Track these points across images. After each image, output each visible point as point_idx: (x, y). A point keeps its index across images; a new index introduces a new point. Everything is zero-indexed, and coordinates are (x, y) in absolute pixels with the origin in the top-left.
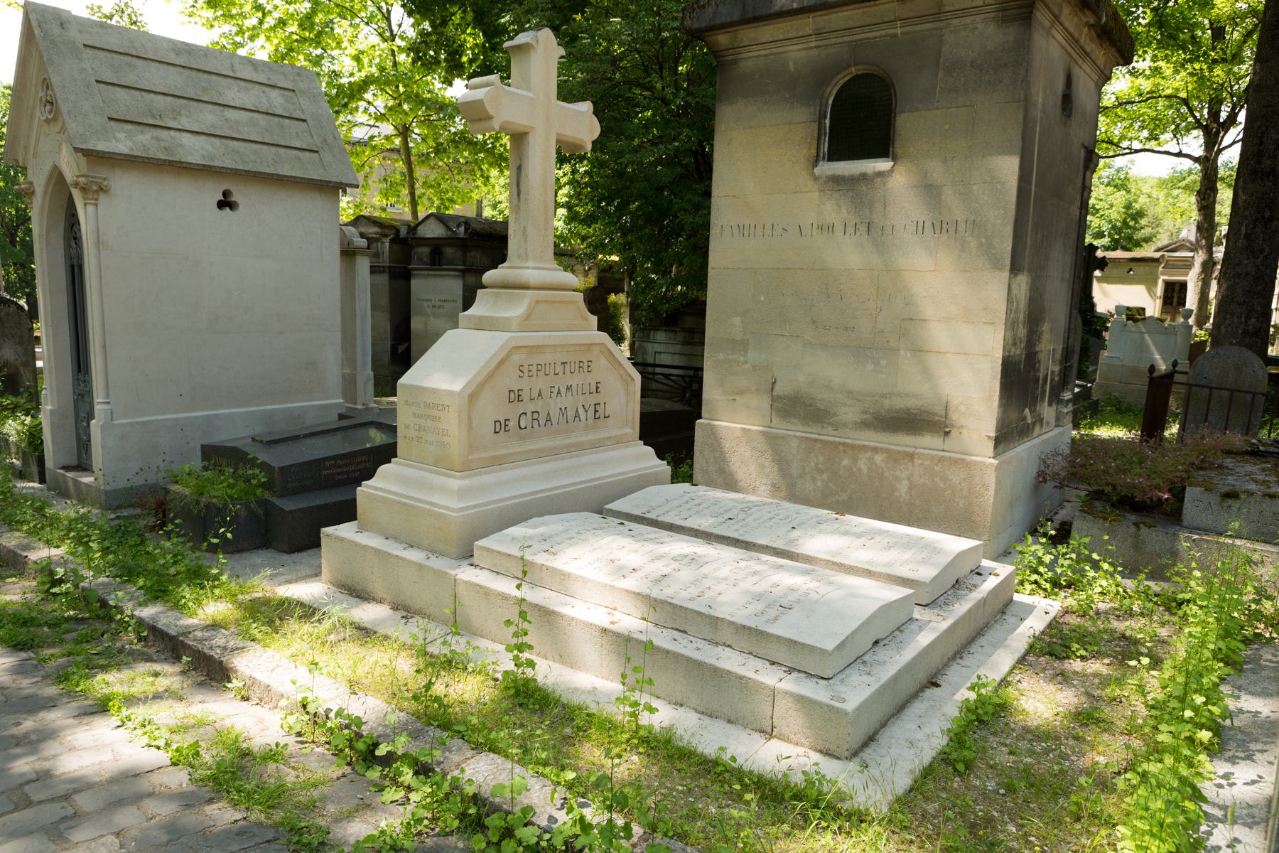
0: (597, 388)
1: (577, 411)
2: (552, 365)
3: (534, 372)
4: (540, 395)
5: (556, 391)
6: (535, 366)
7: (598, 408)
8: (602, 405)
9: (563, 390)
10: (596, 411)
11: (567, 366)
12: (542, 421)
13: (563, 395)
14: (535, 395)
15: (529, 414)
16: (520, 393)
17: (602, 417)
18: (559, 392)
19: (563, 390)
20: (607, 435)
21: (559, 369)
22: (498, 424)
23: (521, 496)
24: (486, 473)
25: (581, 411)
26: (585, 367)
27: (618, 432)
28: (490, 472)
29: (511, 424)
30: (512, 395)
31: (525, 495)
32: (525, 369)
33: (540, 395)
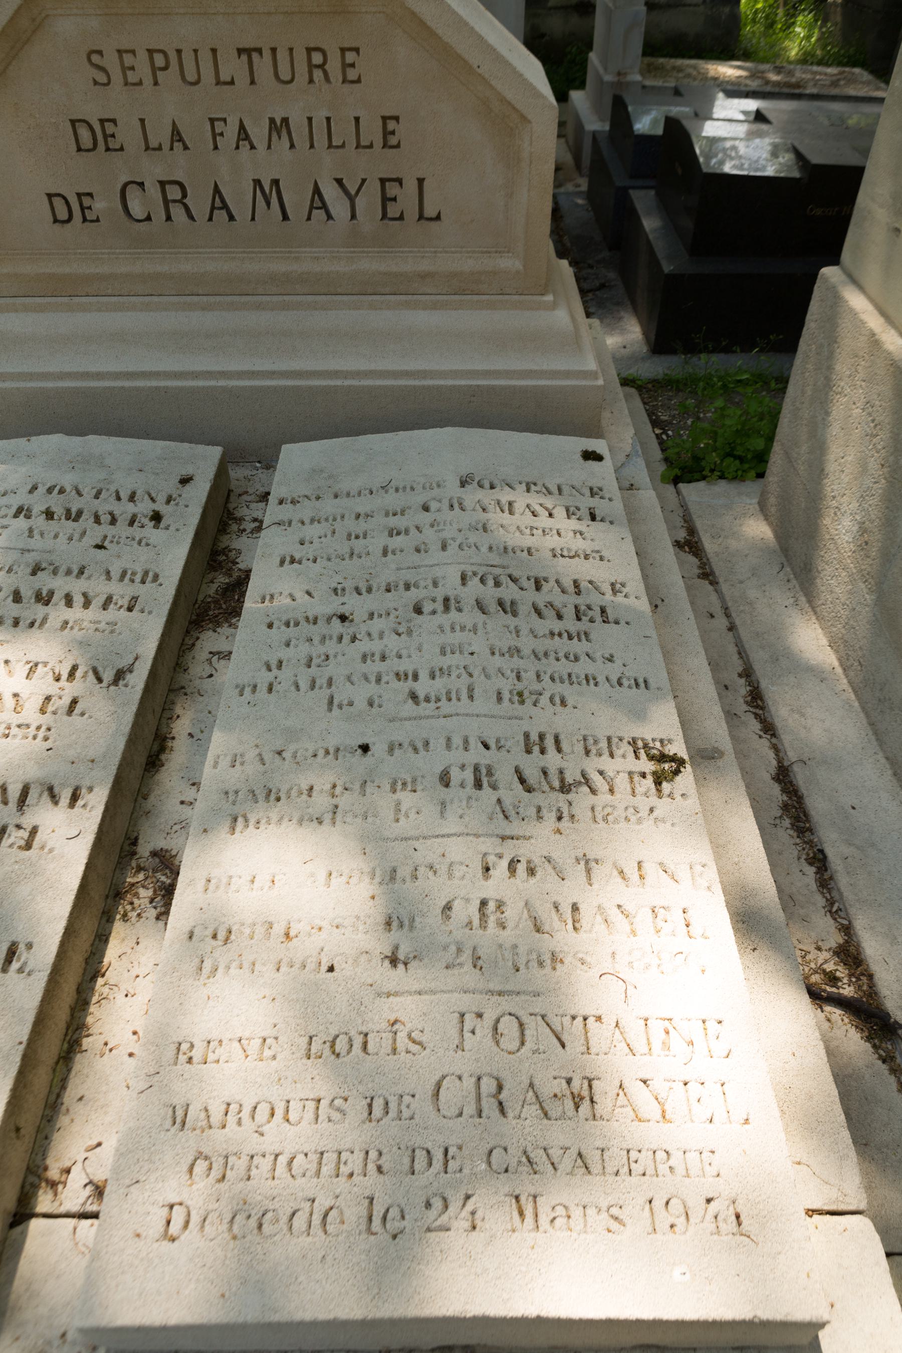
0: (387, 134)
1: (317, 191)
2: (205, 57)
3: (143, 70)
4: (177, 135)
5: (231, 131)
6: (143, 56)
7: (392, 190)
8: (411, 186)
9: (258, 132)
10: (386, 200)
11: (263, 65)
12: (200, 203)
13: (261, 146)
14: (160, 135)
15: (153, 191)
16: (110, 128)
17: (412, 212)
18: (243, 134)
19: (258, 132)
20: (425, 266)
21: (233, 66)
22: (58, 203)
23: (86, 375)
24: (26, 309)
25: (330, 192)
26: (334, 66)
27: (468, 264)
28: (41, 309)
29: (99, 206)
30: (84, 133)
31: (99, 376)
32: (111, 61)
33: (177, 135)
